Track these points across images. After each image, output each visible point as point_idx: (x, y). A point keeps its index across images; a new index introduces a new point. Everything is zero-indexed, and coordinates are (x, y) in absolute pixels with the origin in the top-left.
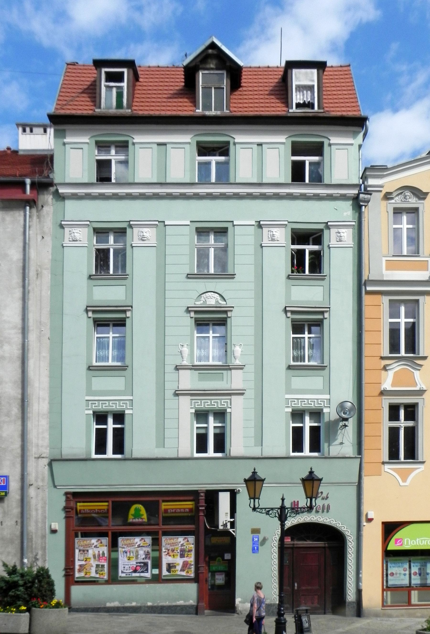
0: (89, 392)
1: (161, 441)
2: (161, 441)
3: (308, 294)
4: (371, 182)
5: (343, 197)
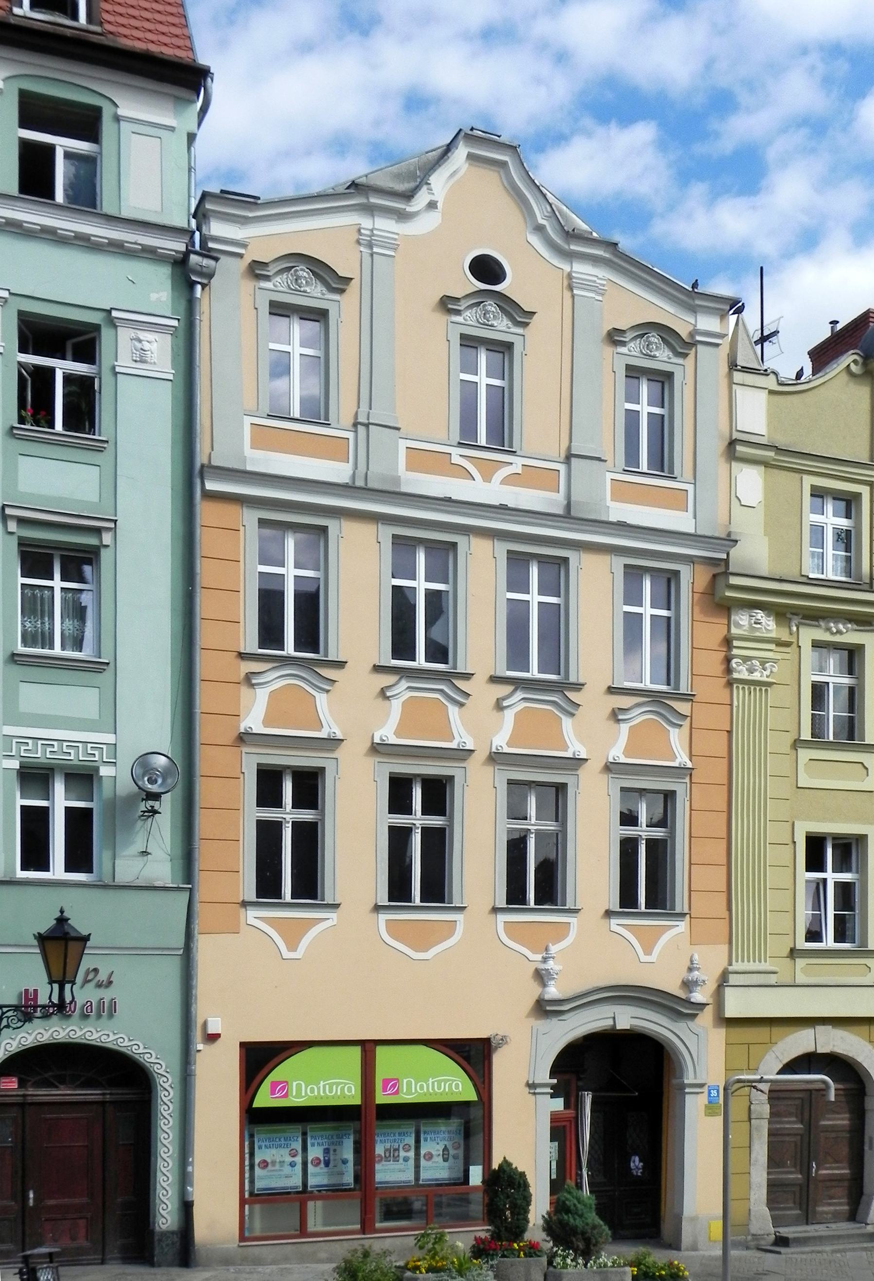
5: (150, 254)
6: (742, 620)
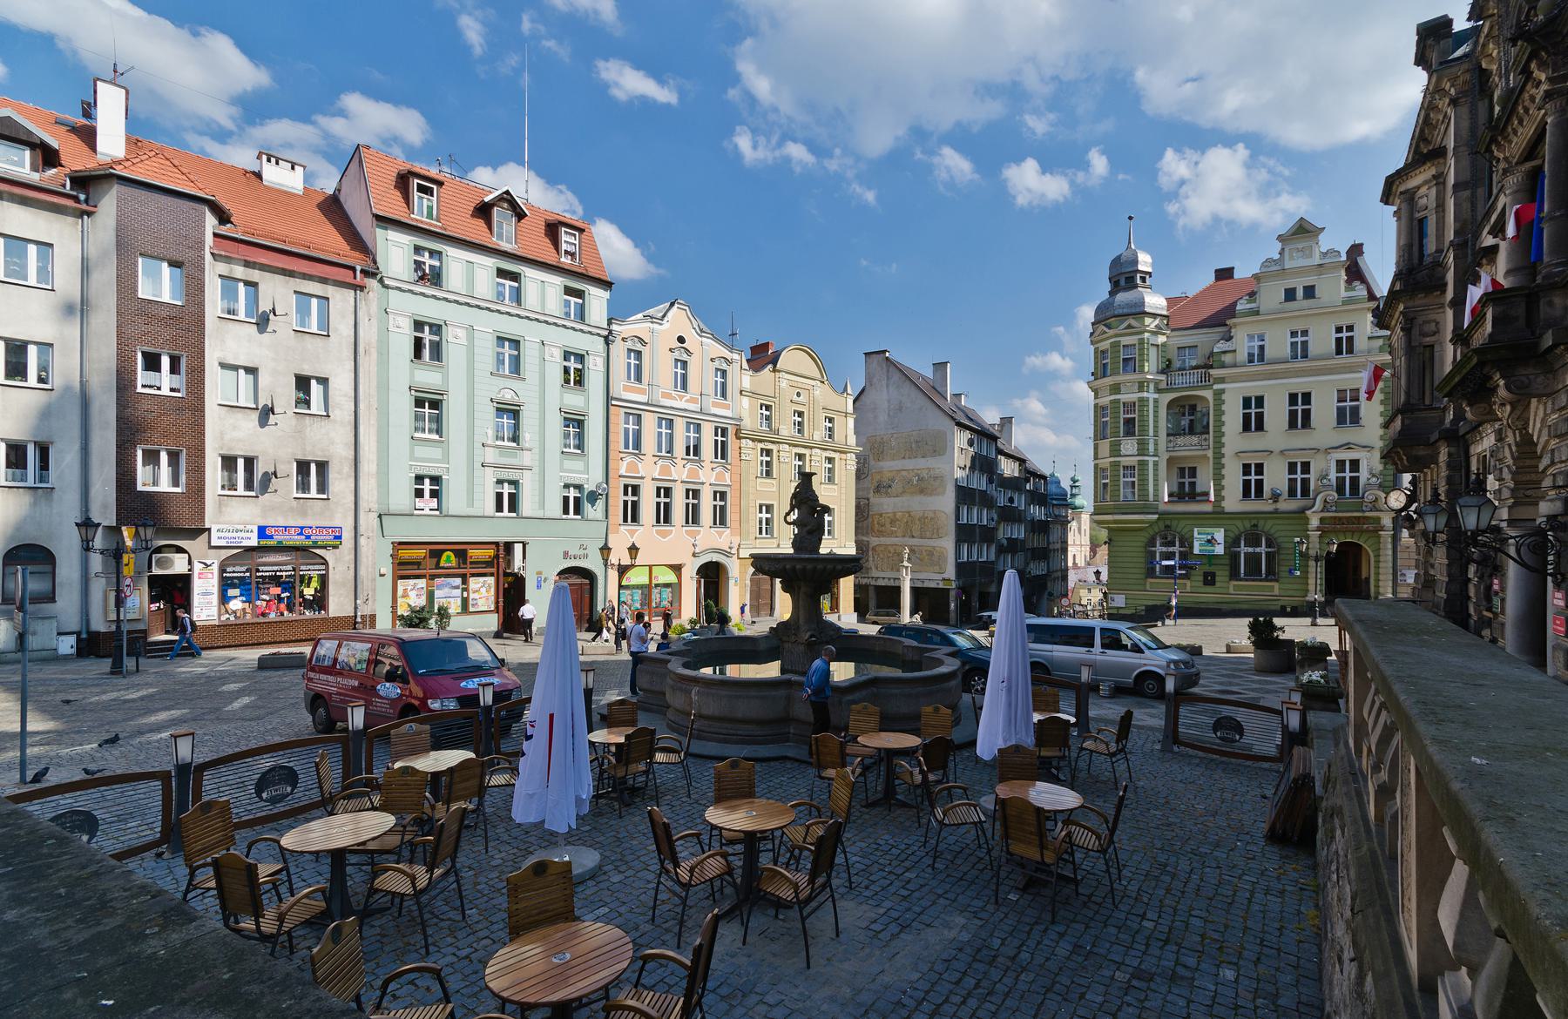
1: (471, 503)
2: (471, 503)
3: (574, 400)
4: (614, 327)
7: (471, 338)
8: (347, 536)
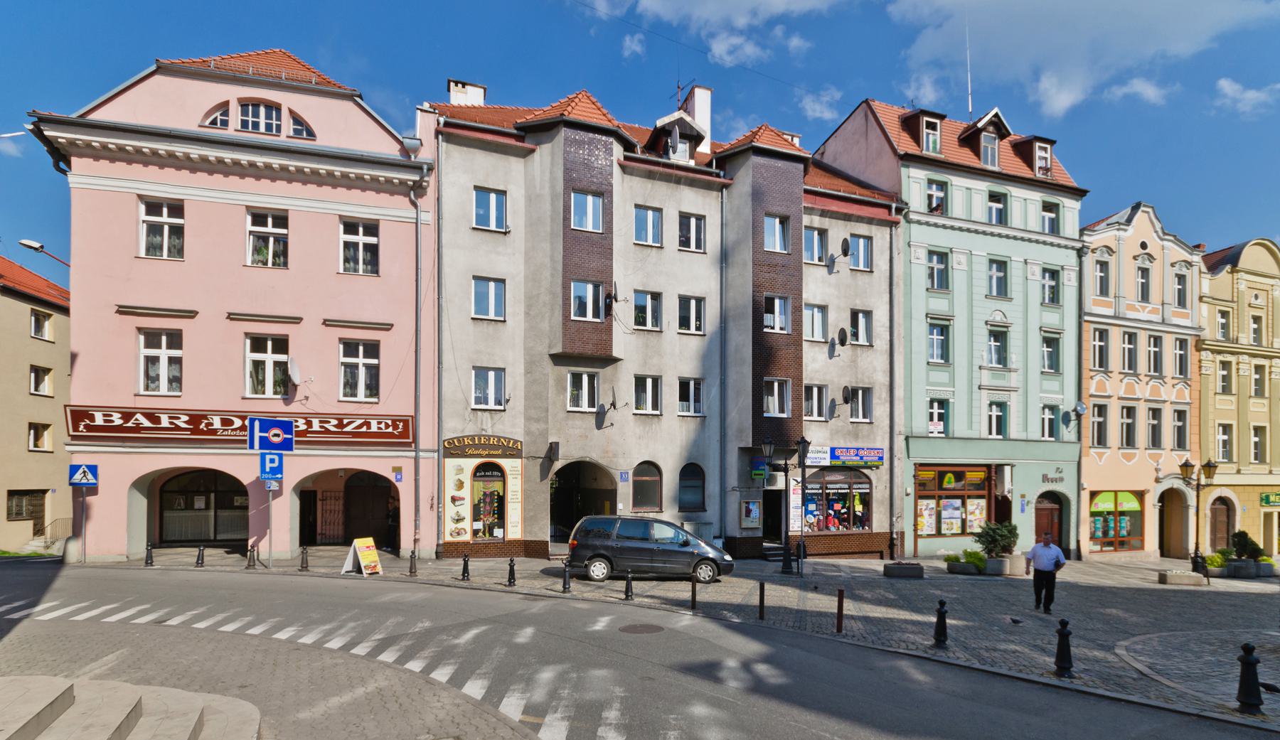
0: (929, 384)
1: (970, 427)
2: (970, 427)
5: (1073, 248)
6: (1203, 353)
7: (970, 263)
8: (886, 456)
